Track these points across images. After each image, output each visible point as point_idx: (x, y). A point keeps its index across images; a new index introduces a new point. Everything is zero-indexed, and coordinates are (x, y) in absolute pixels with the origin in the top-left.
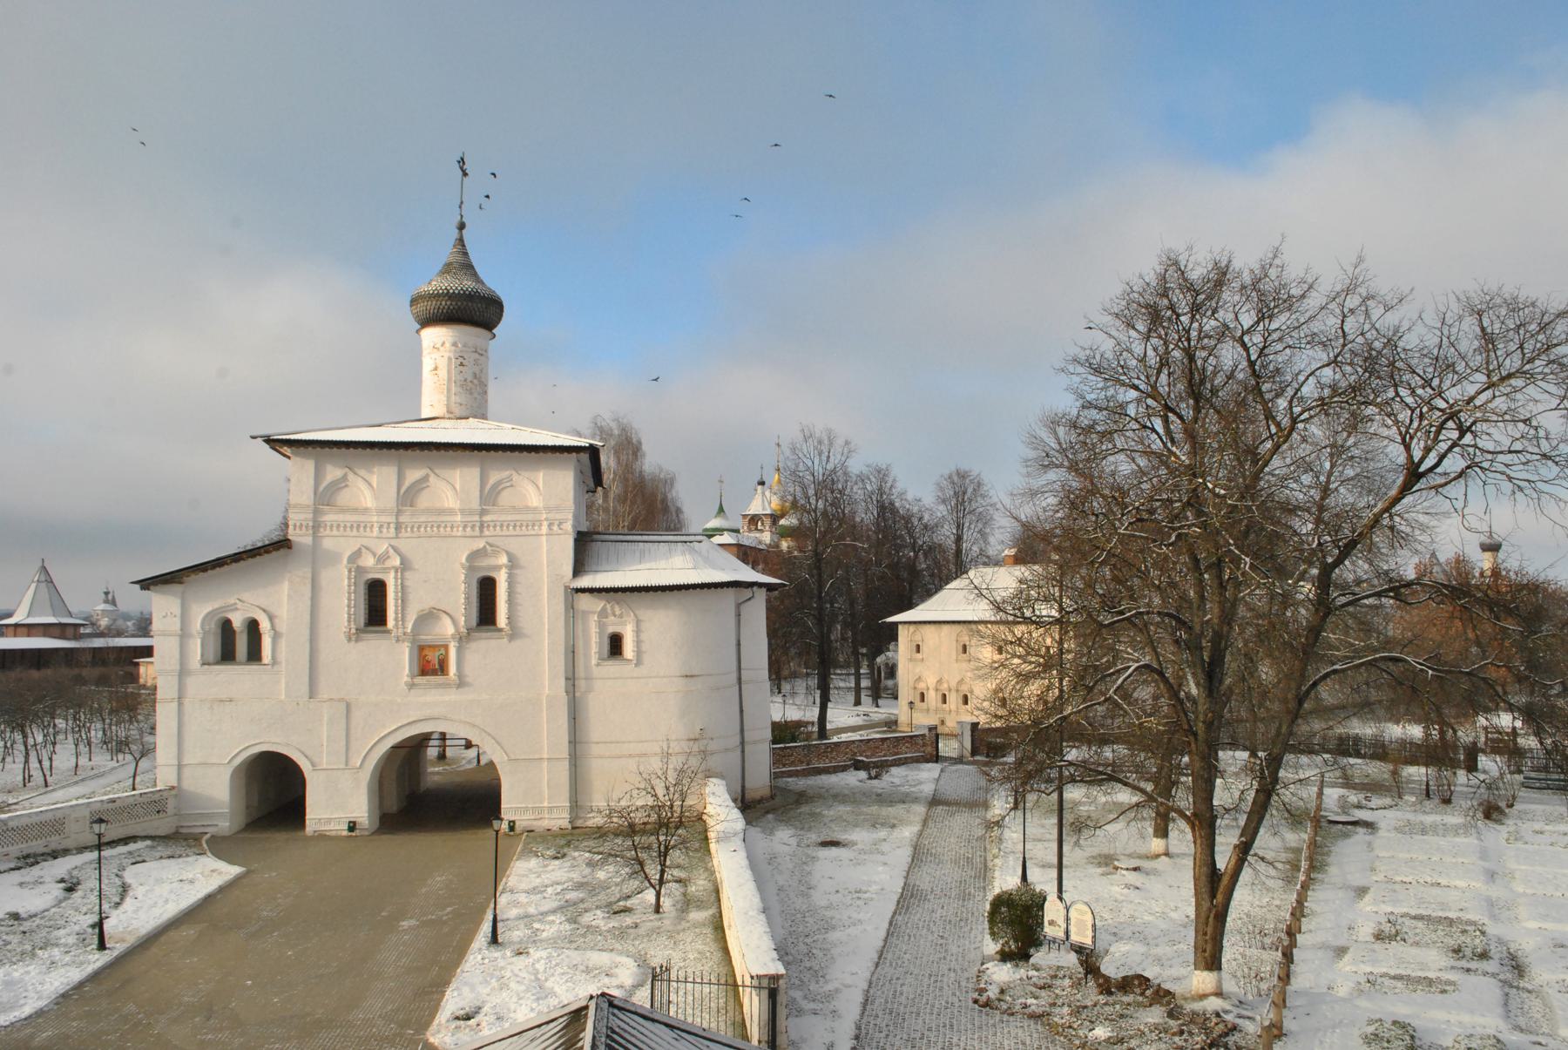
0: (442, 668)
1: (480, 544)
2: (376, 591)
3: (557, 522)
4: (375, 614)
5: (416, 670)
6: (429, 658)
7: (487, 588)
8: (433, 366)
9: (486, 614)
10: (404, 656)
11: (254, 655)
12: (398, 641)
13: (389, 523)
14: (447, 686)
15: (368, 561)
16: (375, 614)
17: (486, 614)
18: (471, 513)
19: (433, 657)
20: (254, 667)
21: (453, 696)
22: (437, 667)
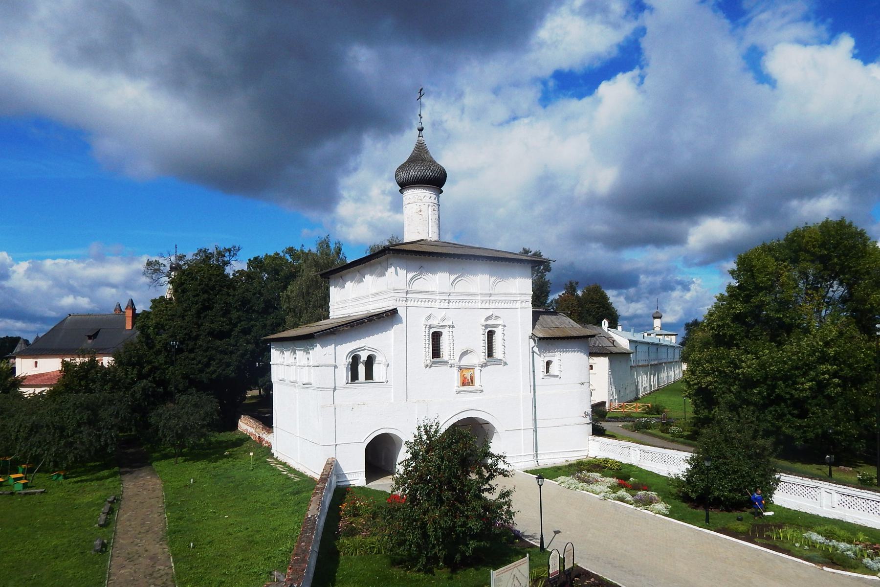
0: (472, 382)
1: (489, 313)
2: (436, 337)
3: (525, 301)
4: (436, 352)
5: (460, 383)
6: (466, 376)
7: (491, 334)
8: (419, 210)
9: (490, 353)
10: (455, 376)
11: (369, 376)
12: (451, 367)
13: (445, 300)
14: (476, 391)
15: (434, 322)
16: (436, 352)
17: (490, 353)
18: (486, 295)
19: (468, 375)
20: (369, 386)
21: (477, 397)
22: (470, 381)
